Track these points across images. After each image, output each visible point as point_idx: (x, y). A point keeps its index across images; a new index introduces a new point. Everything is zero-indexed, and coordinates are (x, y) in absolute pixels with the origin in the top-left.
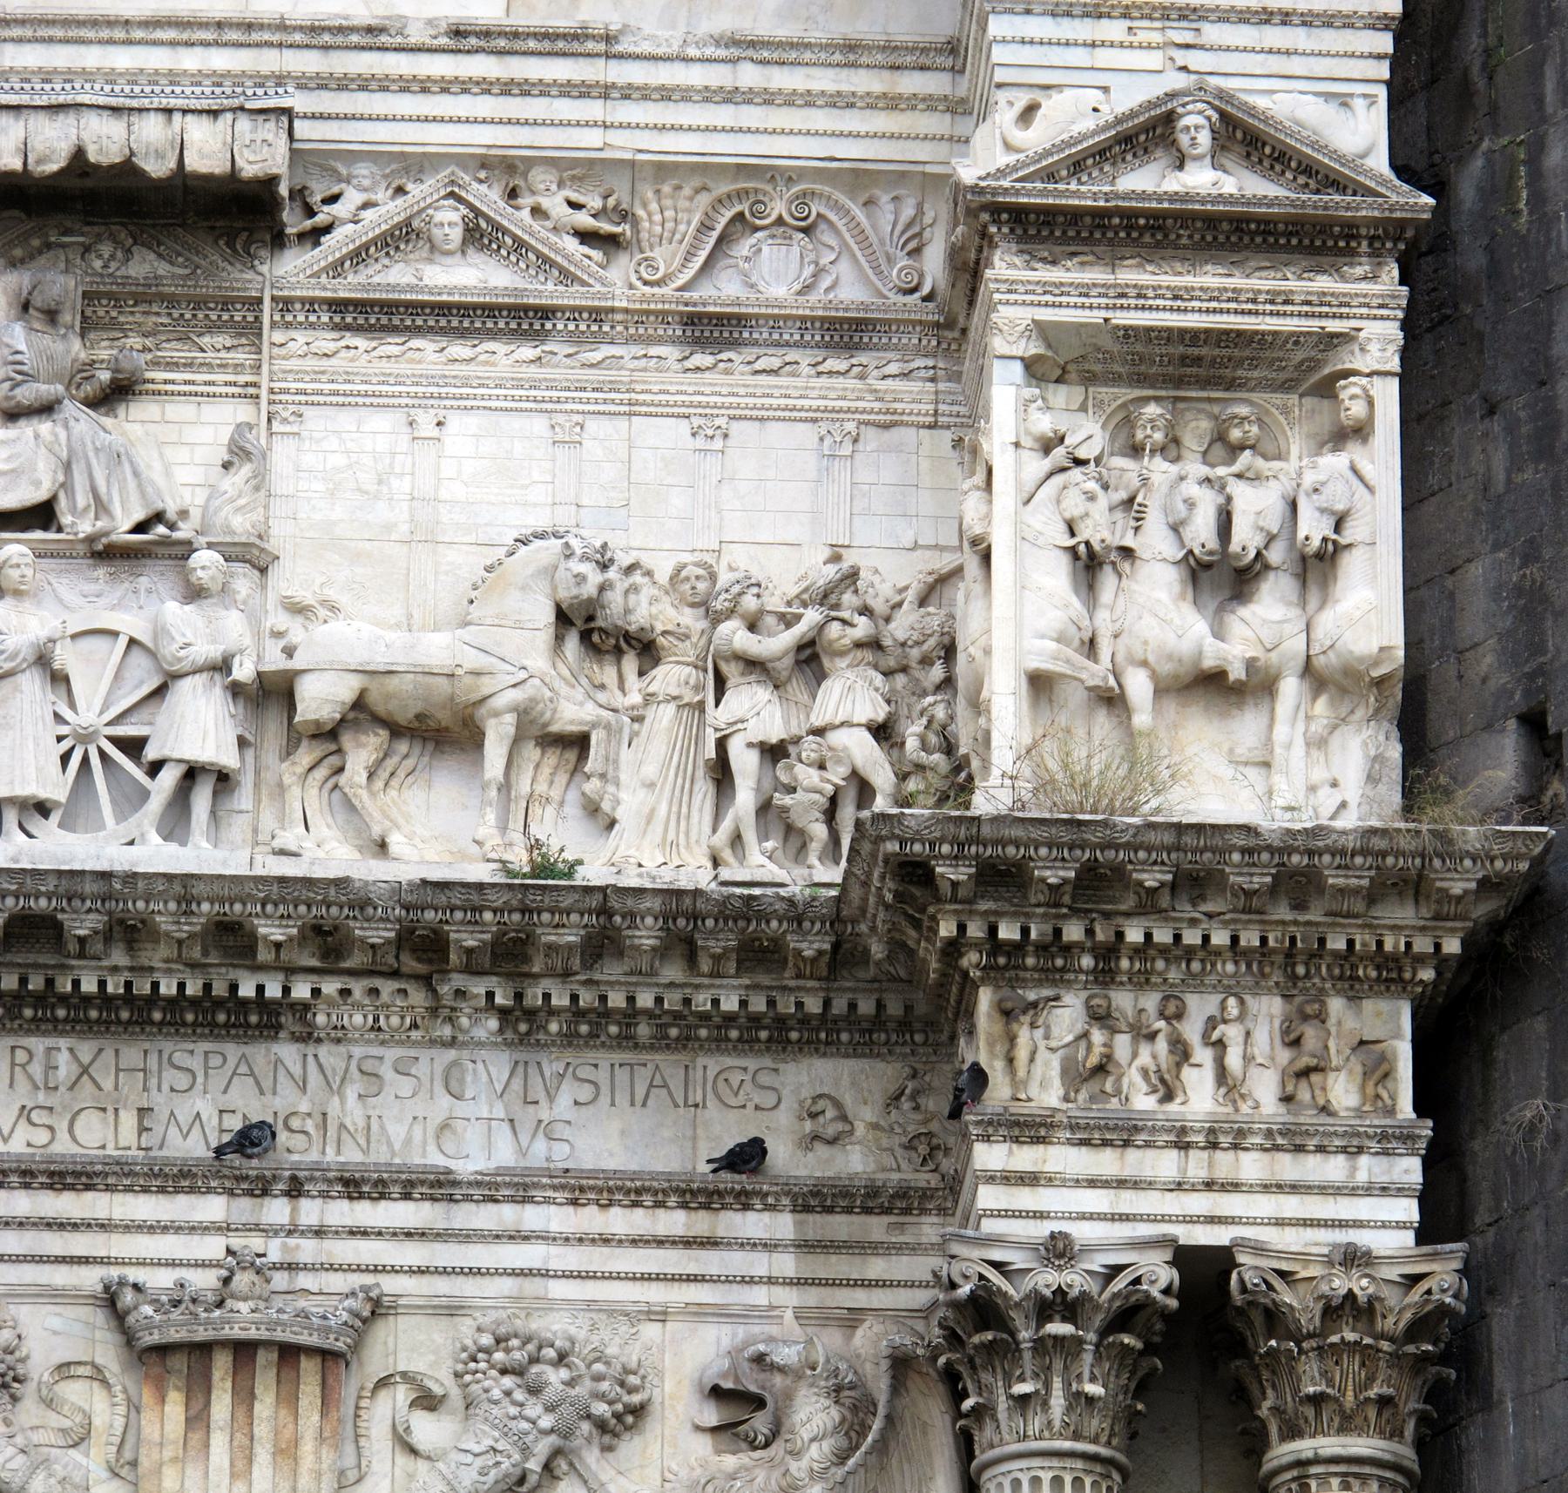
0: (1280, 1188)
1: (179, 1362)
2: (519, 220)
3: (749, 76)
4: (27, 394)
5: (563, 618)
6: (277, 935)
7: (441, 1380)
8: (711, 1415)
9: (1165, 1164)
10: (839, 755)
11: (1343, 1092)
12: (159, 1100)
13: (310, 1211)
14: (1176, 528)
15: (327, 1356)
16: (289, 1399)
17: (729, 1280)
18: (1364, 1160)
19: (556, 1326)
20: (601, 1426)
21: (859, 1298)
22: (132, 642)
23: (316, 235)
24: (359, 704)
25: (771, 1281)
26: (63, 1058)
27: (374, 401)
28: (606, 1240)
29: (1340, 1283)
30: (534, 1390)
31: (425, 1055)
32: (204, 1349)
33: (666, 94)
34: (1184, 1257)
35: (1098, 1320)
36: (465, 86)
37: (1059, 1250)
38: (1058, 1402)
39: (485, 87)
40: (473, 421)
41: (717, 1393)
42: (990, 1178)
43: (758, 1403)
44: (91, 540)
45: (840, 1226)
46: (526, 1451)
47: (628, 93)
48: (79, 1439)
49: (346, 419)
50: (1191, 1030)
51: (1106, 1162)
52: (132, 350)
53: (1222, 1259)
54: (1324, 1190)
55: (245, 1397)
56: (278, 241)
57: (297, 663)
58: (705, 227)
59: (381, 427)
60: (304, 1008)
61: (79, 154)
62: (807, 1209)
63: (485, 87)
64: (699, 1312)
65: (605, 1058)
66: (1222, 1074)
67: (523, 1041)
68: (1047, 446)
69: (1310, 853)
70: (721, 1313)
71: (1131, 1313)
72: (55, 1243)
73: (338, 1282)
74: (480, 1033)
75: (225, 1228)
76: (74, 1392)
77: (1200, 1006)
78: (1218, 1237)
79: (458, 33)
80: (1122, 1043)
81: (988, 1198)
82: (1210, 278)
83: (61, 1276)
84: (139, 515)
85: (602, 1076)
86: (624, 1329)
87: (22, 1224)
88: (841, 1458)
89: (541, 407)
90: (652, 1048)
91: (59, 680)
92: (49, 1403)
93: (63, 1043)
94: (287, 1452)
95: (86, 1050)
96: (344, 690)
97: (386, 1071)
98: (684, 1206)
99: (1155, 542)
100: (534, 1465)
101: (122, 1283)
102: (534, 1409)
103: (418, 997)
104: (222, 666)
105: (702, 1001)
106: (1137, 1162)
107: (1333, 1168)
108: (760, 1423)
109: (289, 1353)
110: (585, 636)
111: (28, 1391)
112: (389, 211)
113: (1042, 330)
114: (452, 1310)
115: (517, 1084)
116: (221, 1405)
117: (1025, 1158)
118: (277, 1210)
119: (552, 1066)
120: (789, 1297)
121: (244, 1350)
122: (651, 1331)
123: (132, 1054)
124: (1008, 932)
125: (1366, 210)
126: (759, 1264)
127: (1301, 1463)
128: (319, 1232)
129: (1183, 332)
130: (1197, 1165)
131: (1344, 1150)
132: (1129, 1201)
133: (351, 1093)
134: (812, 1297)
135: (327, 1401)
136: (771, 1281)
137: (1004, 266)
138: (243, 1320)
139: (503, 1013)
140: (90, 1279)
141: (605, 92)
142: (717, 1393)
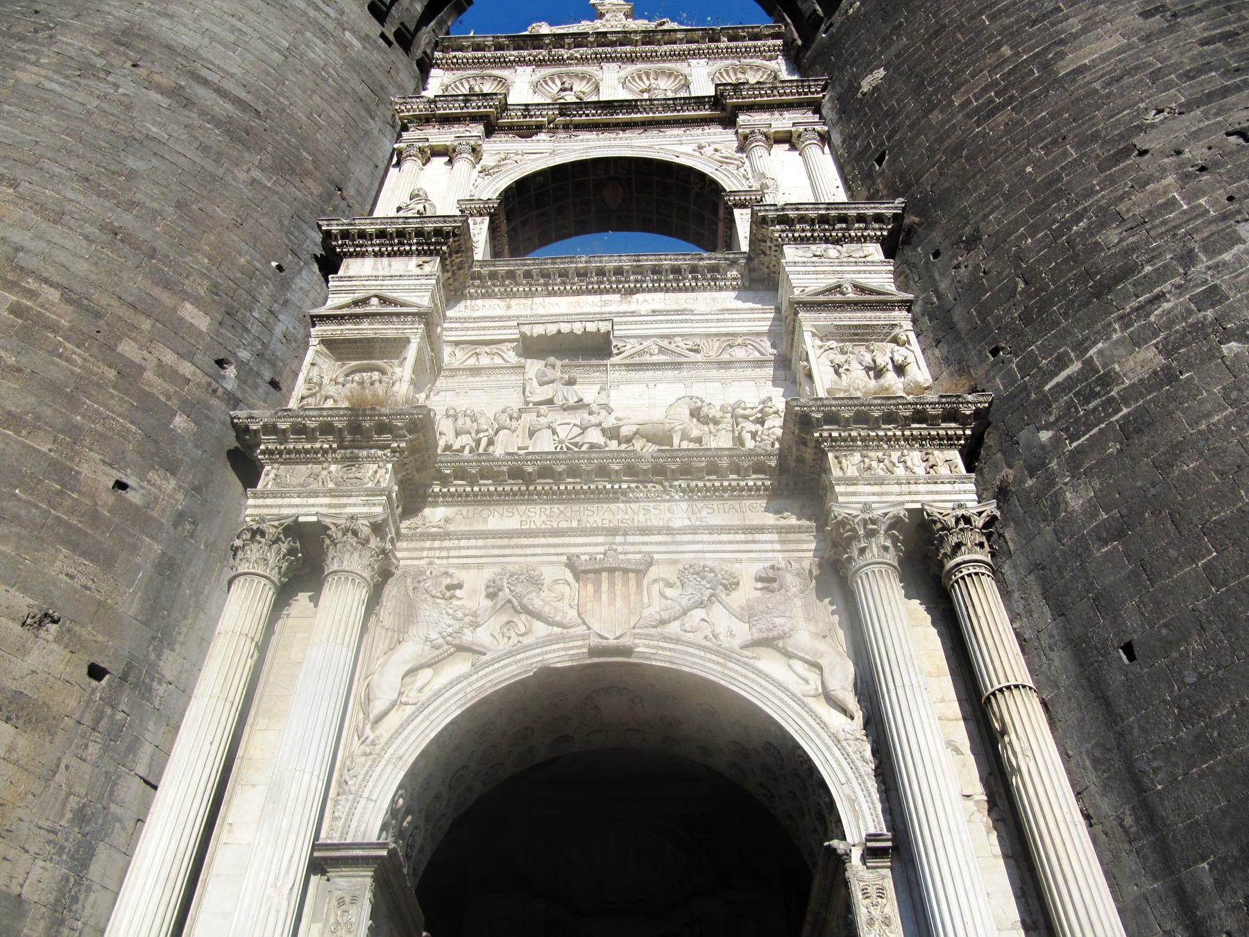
0: (932, 493)
1: (591, 575)
2: (673, 347)
3: (727, 316)
4: (545, 379)
5: (692, 415)
6: (617, 468)
7: (673, 579)
8: (760, 585)
9: (896, 488)
10: (774, 434)
11: (944, 470)
12: (584, 518)
13: (630, 539)
14: (861, 363)
15: (637, 572)
16: (626, 583)
17: (760, 551)
18: (956, 485)
19: (709, 563)
20: (725, 586)
21: (801, 554)
22: (575, 425)
23: (620, 353)
24: (636, 433)
25: (773, 551)
26: (556, 510)
27: (637, 382)
28: (721, 542)
29: (959, 513)
30: (703, 578)
31: (662, 504)
32: (598, 572)
33: (707, 321)
34: (907, 510)
35: (884, 527)
36: (656, 322)
37: (867, 507)
38: (875, 550)
39: (662, 322)
40: (663, 385)
41: (759, 579)
42: (842, 494)
43: (774, 580)
44: (563, 405)
45: (792, 536)
46: (702, 594)
47: (697, 321)
48: (561, 599)
49: (631, 386)
50: (896, 461)
51: (876, 489)
52: (575, 373)
53: (922, 510)
54: (946, 493)
55: (612, 585)
56: (610, 355)
57: (620, 423)
58: (719, 347)
59: (640, 388)
60: (624, 493)
61: (559, 332)
62: (781, 533)
63: (662, 322)
64: (752, 560)
65: (715, 503)
66: (907, 468)
67: (691, 499)
68: (821, 347)
69: (922, 404)
70: (758, 560)
71: (896, 523)
72: (552, 550)
73: (639, 556)
74: (677, 497)
75: (602, 544)
76: (560, 588)
77: (895, 455)
78: (918, 506)
79: (654, 311)
80: (874, 464)
81: (841, 499)
82: (859, 314)
83: (554, 558)
84: (576, 400)
85: (715, 507)
86: (729, 565)
87: (542, 546)
88: (802, 592)
89: (681, 381)
90: (728, 500)
91: (554, 432)
92: (550, 590)
93: (556, 506)
94: (626, 598)
95: (562, 507)
96: (634, 428)
97: (651, 508)
98: (744, 533)
99: (855, 365)
100: (705, 598)
101: (573, 555)
102: (704, 582)
103: (659, 487)
104: (600, 424)
105: (743, 483)
106: (885, 488)
107: (948, 487)
108: (775, 585)
109: (625, 571)
110: (698, 420)
111: (545, 588)
112: (639, 348)
113: (814, 326)
114: (675, 562)
115: (690, 509)
116: (605, 587)
117: (852, 489)
118: (619, 539)
119: (700, 504)
120: (779, 555)
121: (611, 571)
122: (738, 565)
123: (575, 508)
124: (835, 434)
125: (895, 298)
126: (768, 547)
127: (958, 565)
128: (633, 544)
129: (853, 326)
130: (905, 488)
131: (949, 483)
132: (885, 498)
133: (641, 514)
134: (786, 555)
135: (639, 584)
136: (773, 551)
137: (802, 315)
138: (610, 562)
139: (684, 491)
140: (564, 558)
141: (692, 321)
142: (759, 579)
